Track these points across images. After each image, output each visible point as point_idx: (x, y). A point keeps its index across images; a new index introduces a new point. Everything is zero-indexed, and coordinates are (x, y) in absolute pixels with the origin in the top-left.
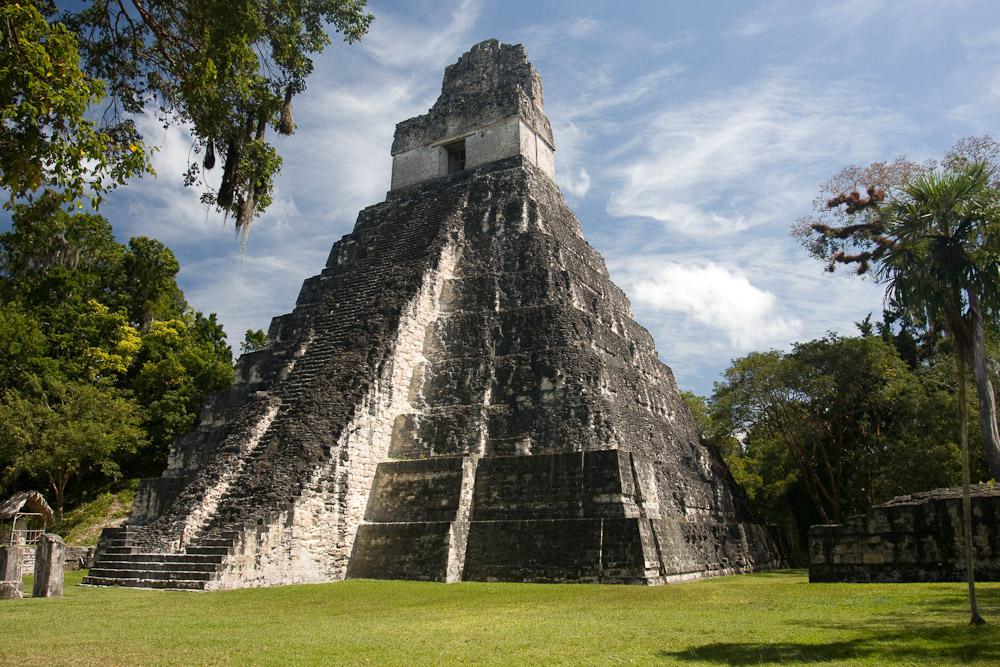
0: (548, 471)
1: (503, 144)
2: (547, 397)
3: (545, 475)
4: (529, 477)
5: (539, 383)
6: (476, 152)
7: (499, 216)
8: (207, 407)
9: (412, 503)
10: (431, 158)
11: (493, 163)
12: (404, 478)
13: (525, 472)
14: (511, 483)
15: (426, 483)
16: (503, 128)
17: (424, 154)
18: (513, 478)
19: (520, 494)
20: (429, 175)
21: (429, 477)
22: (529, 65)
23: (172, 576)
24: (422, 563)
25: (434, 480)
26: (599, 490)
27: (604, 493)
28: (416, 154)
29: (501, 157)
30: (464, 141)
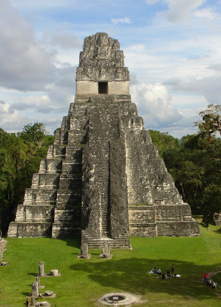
1: (123, 89)
2: (165, 189)
4: (168, 211)
5: (163, 185)
6: (112, 89)
7: (134, 123)
8: (34, 179)
9: (140, 218)
10: (94, 86)
11: (120, 95)
12: (136, 211)
13: (167, 210)
14: (164, 212)
15: (144, 213)
16: (123, 83)
17: (91, 83)
18: (164, 211)
19: (167, 215)
20: (94, 92)
21: (144, 211)
22: (122, 52)
23: (116, 246)
24: (149, 234)
25: (146, 212)
26: (186, 214)
27: (187, 215)
28: (87, 82)
30: (107, 83)
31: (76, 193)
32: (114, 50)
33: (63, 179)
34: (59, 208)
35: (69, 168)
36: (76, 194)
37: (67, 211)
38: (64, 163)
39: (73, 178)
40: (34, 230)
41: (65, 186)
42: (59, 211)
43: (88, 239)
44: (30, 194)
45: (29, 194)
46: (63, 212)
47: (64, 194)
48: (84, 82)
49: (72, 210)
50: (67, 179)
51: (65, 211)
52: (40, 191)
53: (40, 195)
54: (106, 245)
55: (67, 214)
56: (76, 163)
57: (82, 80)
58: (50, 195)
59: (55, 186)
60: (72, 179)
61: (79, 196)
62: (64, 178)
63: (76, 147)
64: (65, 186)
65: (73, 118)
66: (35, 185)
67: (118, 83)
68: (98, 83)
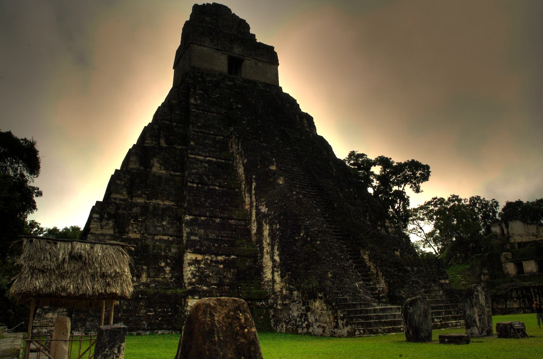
0: (422, 266)
2: (390, 230)
3: (421, 268)
4: (415, 269)
26: (441, 277)
28: (210, 51)
29: (268, 82)
31: (235, 219)
32: (242, 30)
33: (195, 185)
34: (200, 250)
35: (205, 167)
36: (233, 221)
37: (220, 258)
38: (193, 156)
39: (218, 186)
40: (125, 311)
41: (200, 202)
42: (200, 257)
43: (356, 304)
44: (109, 214)
45: (106, 216)
46: (211, 261)
47: (203, 218)
48: (205, 49)
49: (233, 257)
50: (206, 188)
51: (214, 259)
52: (135, 210)
53: (136, 218)
54: (480, 297)
55: (222, 266)
56: (220, 160)
57: (200, 45)
58: (163, 220)
59: (173, 203)
60: (217, 188)
61: (240, 225)
62: (197, 184)
63: (212, 132)
64: (200, 202)
65: (197, 88)
66: (118, 196)
67: (260, 64)
68: (229, 57)
